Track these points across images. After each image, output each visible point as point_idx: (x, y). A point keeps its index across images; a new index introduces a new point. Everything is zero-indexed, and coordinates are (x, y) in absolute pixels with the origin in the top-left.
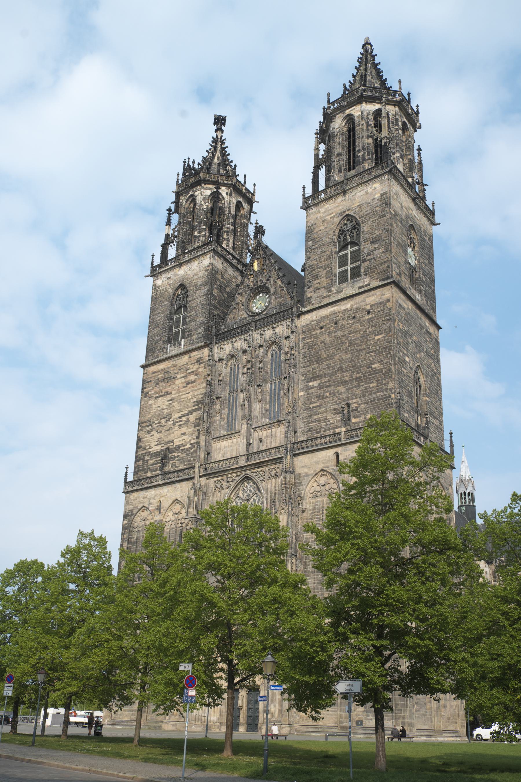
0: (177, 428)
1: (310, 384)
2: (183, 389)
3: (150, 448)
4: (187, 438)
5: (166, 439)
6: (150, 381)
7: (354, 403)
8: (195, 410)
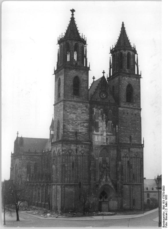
0: (79, 126)
1: (121, 127)
3: (69, 129)
4: (84, 131)
5: (76, 129)
7: (132, 136)
8: (86, 123)
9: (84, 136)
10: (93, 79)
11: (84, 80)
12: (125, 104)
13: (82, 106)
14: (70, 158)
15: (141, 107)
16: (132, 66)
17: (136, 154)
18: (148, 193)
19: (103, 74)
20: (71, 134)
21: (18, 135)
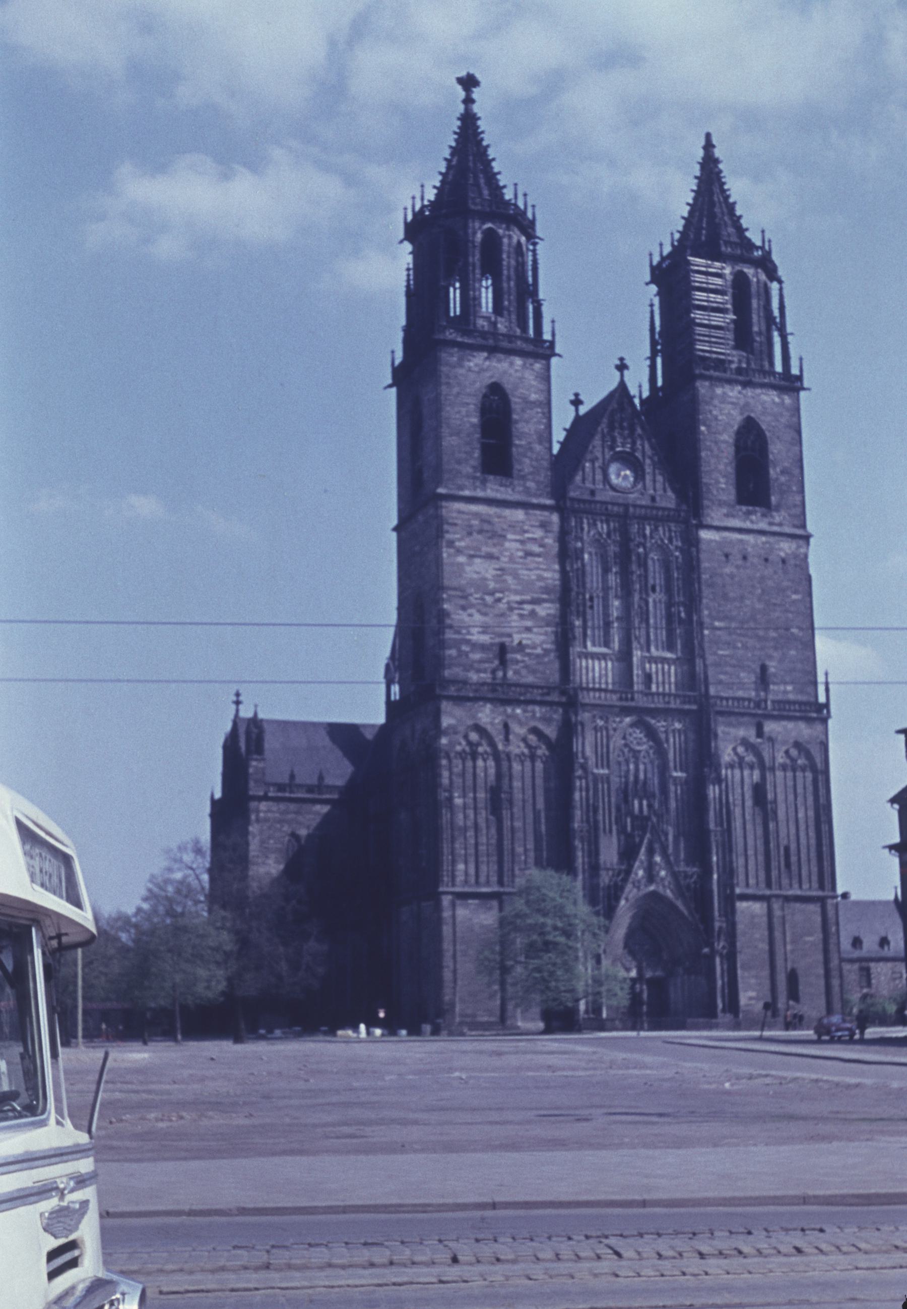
0: (515, 617)
1: (717, 624)
2: (521, 560)
3: (469, 633)
4: (538, 639)
6: (455, 525)
8: (545, 601)
9: (539, 663)
10: (573, 408)
11: (529, 404)
12: (727, 515)
13: (523, 522)
14: (475, 767)
15: (810, 527)
16: (760, 333)
17: (794, 752)
18: (864, 964)
19: (618, 374)
20: (477, 656)
21: (237, 711)
